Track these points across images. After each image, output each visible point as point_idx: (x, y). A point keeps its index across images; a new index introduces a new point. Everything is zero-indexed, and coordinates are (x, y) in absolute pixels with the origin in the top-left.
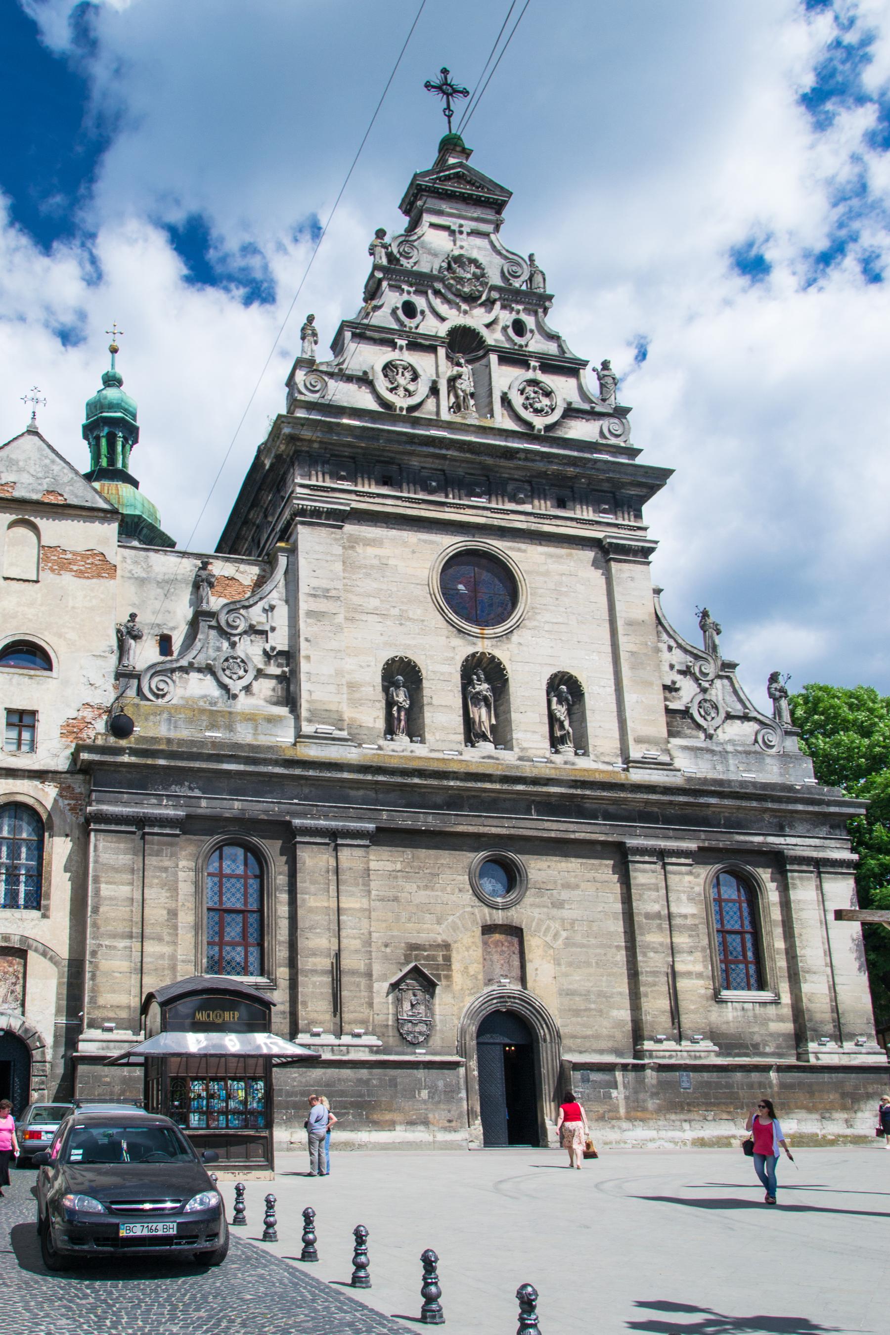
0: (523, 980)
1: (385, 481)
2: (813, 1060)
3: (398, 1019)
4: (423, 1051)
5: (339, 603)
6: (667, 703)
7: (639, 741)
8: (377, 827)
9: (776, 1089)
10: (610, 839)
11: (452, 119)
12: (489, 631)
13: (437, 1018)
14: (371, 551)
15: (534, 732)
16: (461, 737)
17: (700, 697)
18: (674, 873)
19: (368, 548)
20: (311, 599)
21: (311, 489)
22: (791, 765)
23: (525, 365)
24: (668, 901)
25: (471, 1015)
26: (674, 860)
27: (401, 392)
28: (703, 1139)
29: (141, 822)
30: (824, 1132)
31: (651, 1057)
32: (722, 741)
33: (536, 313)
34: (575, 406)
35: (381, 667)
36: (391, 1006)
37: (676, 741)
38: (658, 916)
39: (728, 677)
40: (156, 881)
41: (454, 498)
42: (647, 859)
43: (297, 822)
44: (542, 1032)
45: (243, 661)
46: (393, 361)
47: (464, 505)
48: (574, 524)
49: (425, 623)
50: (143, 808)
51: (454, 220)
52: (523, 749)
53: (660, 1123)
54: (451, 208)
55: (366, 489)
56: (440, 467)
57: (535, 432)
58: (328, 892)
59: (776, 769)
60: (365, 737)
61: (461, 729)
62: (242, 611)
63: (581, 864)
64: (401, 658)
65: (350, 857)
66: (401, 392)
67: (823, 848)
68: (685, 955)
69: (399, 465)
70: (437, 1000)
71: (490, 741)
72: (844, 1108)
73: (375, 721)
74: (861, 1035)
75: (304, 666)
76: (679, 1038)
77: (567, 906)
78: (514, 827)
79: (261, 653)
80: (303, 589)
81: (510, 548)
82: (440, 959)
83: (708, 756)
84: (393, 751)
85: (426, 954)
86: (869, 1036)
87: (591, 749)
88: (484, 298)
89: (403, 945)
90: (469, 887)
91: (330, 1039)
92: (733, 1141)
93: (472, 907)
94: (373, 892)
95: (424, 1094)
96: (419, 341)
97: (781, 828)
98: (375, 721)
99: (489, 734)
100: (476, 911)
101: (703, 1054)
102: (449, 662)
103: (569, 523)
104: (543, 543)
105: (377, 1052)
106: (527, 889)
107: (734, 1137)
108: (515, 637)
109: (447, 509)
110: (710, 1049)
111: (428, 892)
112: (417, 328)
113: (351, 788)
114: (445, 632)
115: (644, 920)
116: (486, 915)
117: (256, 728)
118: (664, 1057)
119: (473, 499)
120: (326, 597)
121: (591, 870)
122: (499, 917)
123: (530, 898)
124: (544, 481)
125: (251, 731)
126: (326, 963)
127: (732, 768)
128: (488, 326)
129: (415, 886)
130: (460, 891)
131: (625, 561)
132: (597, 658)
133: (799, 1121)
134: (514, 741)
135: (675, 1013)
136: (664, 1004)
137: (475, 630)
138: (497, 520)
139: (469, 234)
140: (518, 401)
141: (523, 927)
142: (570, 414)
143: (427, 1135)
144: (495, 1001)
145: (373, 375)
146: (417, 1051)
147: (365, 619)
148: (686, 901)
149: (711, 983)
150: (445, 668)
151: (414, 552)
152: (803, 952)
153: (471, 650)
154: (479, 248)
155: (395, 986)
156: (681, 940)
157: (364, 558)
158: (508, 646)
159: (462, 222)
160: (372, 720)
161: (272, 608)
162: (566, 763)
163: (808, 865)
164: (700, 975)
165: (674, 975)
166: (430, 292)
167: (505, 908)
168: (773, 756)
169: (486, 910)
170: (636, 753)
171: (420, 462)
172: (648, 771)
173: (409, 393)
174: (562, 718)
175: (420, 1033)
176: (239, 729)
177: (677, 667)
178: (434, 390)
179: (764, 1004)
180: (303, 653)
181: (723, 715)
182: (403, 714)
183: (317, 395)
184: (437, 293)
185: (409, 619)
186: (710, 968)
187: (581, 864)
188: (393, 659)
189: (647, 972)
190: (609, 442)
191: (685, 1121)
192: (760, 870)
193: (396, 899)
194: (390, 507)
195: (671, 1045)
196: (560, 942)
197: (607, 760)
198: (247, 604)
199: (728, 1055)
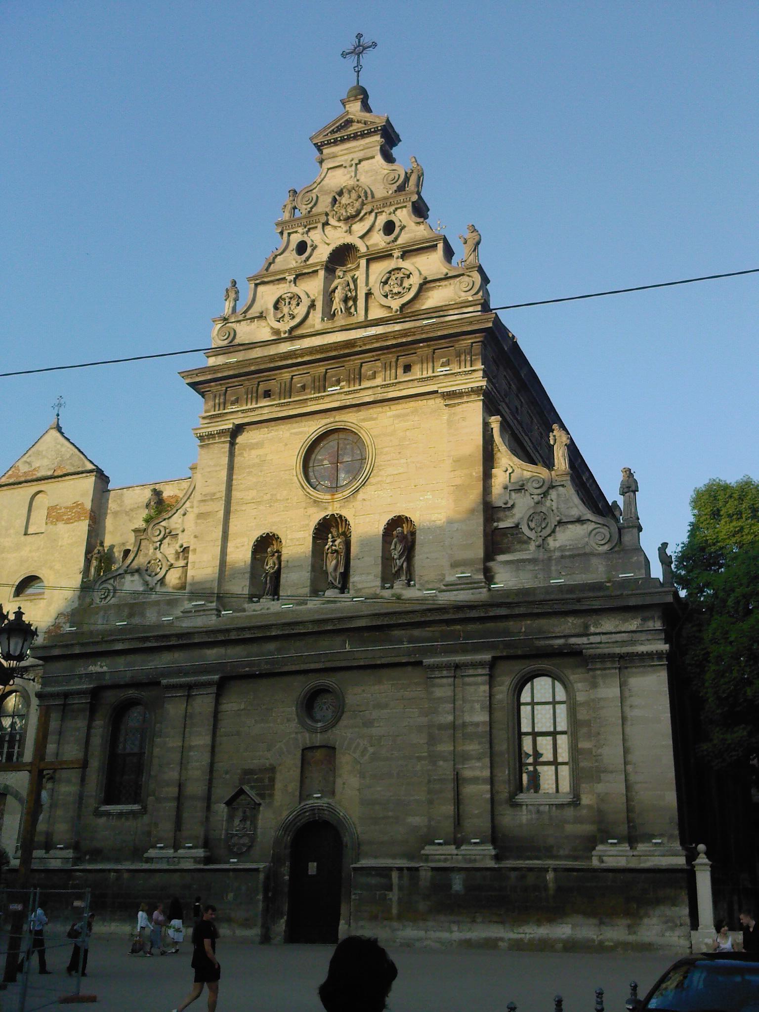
0: (333, 793)
1: (267, 394)
2: (595, 863)
3: (228, 834)
4: (235, 860)
5: (221, 502)
6: (495, 524)
7: (455, 565)
8: (221, 678)
9: (551, 892)
10: (412, 660)
11: (360, 73)
12: (339, 496)
13: (259, 831)
14: (254, 453)
15: (368, 574)
16: (307, 590)
17: (532, 511)
18: (469, 684)
19: (252, 451)
20: (202, 504)
21: (210, 419)
22: (621, 561)
23: (391, 256)
24: (463, 712)
25: (286, 827)
26: (471, 672)
27: (287, 318)
28: (470, 940)
29: (66, 695)
30: (601, 937)
31: (427, 860)
32: (552, 549)
33: (405, 207)
34: (429, 279)
35: (252, 544)
36: (224, 823)
37: (501, 558)
38: (454, 726)
39: (563, 486)
40: (72, 739)
41: (314, 394)
42: (445, 673)
43: (164, 682)
44: (346, 839)
45: (160, 561)
46: (281, 296)
47: (322, 396)
48: (416, 384)
49: (289, 501)
50: (73, 686)
51: (346, 157)
52: (358, 590)
53: (430, 924)
54: (342, 150)
55: (249, 406)
56: (305, 372)
57: (394, 314)
58: (184, 734)
59: (602, 569)
60: (234, 604)
61: (309, 584)
62: (163, 524)
63: (392, 685)
64: (268, 534)
65: (203, 704)
66: (287, 318)
67: (633, 642)
68: (473, 761)
69: (275, 379)
70: (260, 817)
71: (336, 588)
72: (627, 913)
73: (243, 590)
74: (661, 836)
75: (191, 557)
76: (458, 843)
77: (376, 725)
78: (329, 661)
79: (174, 552)
80: (197, 496)
81: (364, 420)
82: (266, 781)
83: (530, 567)
84: (254, 611)
85: (255, 777)
86: (671, 837)
87: (417, 579)
88: (362, 215)
89: (239, 771)
90: (294, 716)
91: (170, 852)
92: (500, 944)
93: (296, 733)
94: (222, 730)
95: (231, 896)
96: (304, 271)
97: (587, 627)
98: (243, 590)
99: (336, 584)
100: (299, 736)
101: (478, 857)
102: (305, 529)
103: (410, 385)
104: (392, 407)
105: (199, 863)
106: (343, 713)
107: (502, 939)
108: (361, 495)
109: (309, 403)
110: (486, 852)
111: (262, 725)
112: (308, 259)
113: (208, 648)
114: (304, 505)
115: (437, 732)
116: (307, 738)
117: (158, 613)
118: (439, 861)
119: (329, 390)
120: (212, 500)
121: (401, 689)
122: (318, 739)
123: (344, 722)
124: (390, 356)
125: (156, 615)
126: (173, 791)
127: (554, 574)
128: (362, 237)
129: (253, 721)
130: (288, 720)
131: (459, 404)
132: (431, 497)
133: (574, 926)
134: (351, 584)
135: (458, 819)
136: (449, 809)
137: (328, 497)
138: (349, 400)
139: (356, 164)
140: (377, 291)
141: (336, 747)
142: (428, 286)
143: (229, 931)
144: (307, 814)
145: (266, 312)
146: (232, 860)
147: (243, 509)
148: (479, 710)
149: (507, 786)
150: (300, 535)
151: (286, 445)
152: (600, 750)
153: (322, 515)
154: (367, 172)
155: (229, 803)
156: (473, 747)
157: (249, 460)
158: (354, 504)
159: (350, 157)
160: (241, 589)
161: (184, 515)
162: (393, 596)
163: (613, 662)
164: (484, 781)
165: (458, 781)
166: (320, 226)
167: (324, 730)
168: (599, 554)
169: (307, 735)
170: (450, 578)
171: (289, 372)
172: (454, 592)
173: (293, 317)
174: (396, 557)
175: (244, 845)
176: (148, 615)
177: (510, 488)
178: (312, 306)
179: (561, 806)
180: (191, 548)
181: (553, 521)
182: (268, 578)
183: (226, 342)
184: (326, 224)
185: (277, 500)
186: (507, 772)
187: (392, 685)
188: (261, 536)
189: (435, 780)
190: (459, 300)
191: (454, 922)
192: (568, 672)
193: (238, 733)
194: (266, 414)
195: (452, 849)
196: (367, 757)
197: (430, 587)
198: (167, 517)
199: (518, 858)
